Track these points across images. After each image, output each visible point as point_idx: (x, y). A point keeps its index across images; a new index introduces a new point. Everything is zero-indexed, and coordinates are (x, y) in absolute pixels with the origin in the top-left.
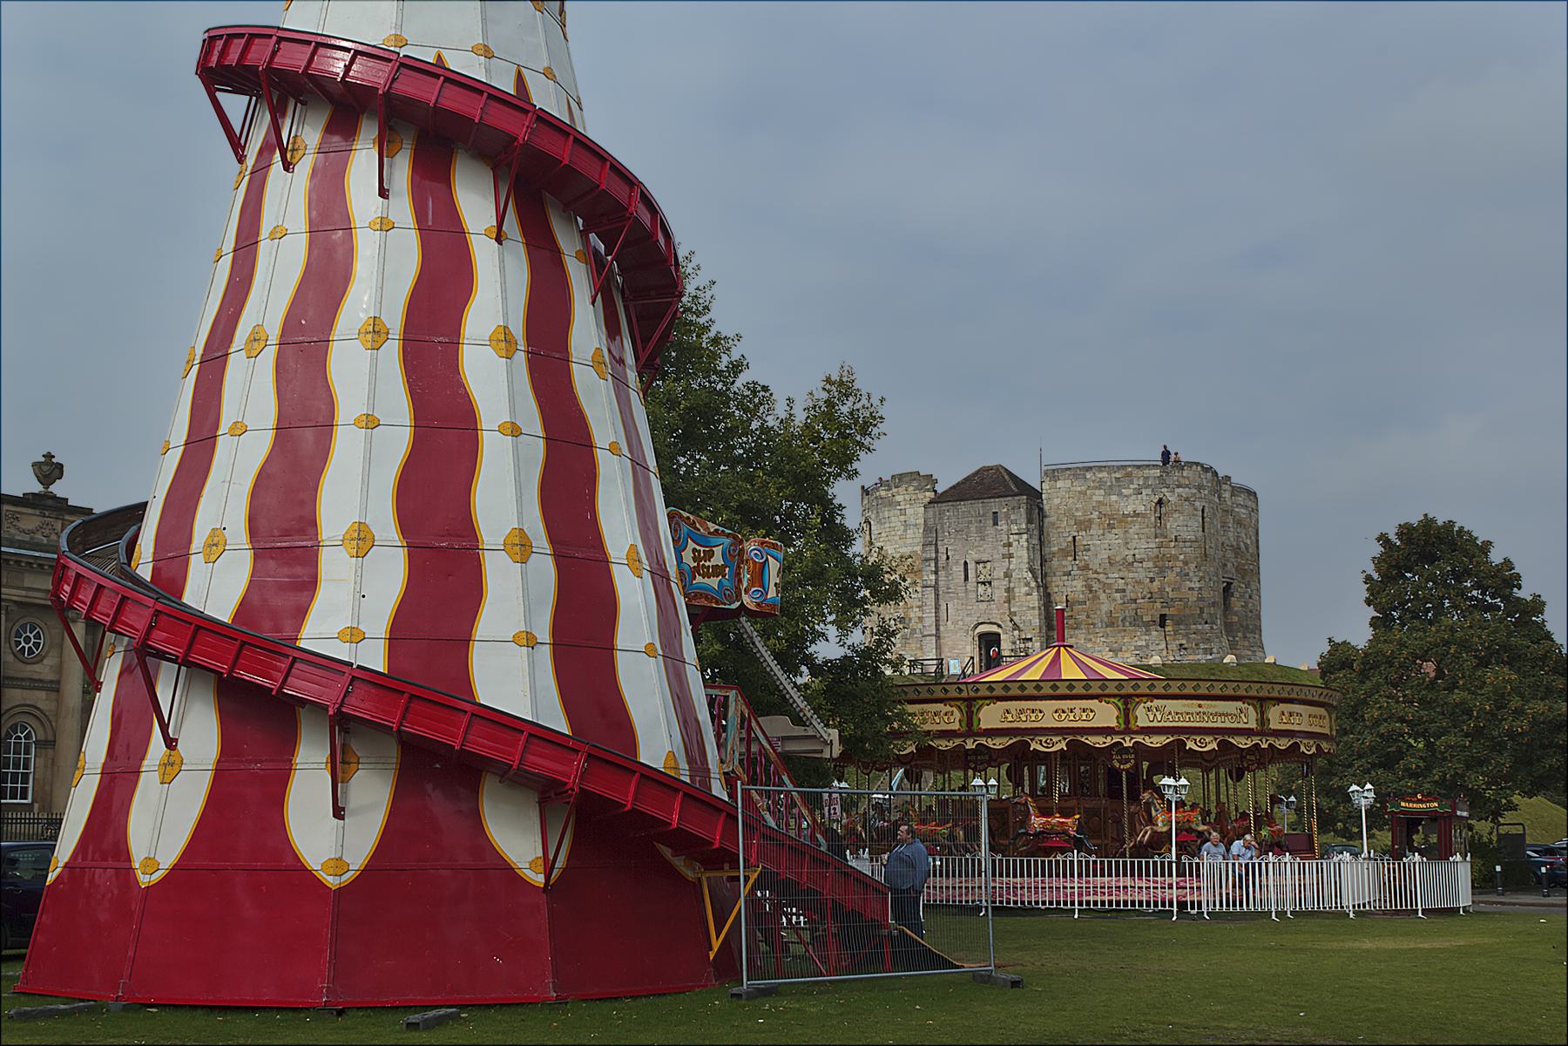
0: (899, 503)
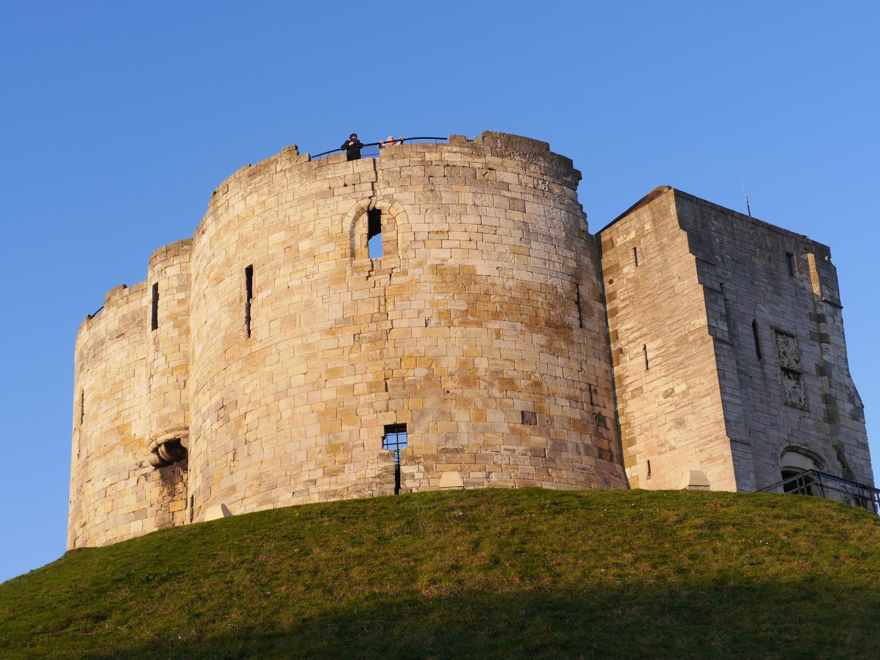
0: (506, 186)
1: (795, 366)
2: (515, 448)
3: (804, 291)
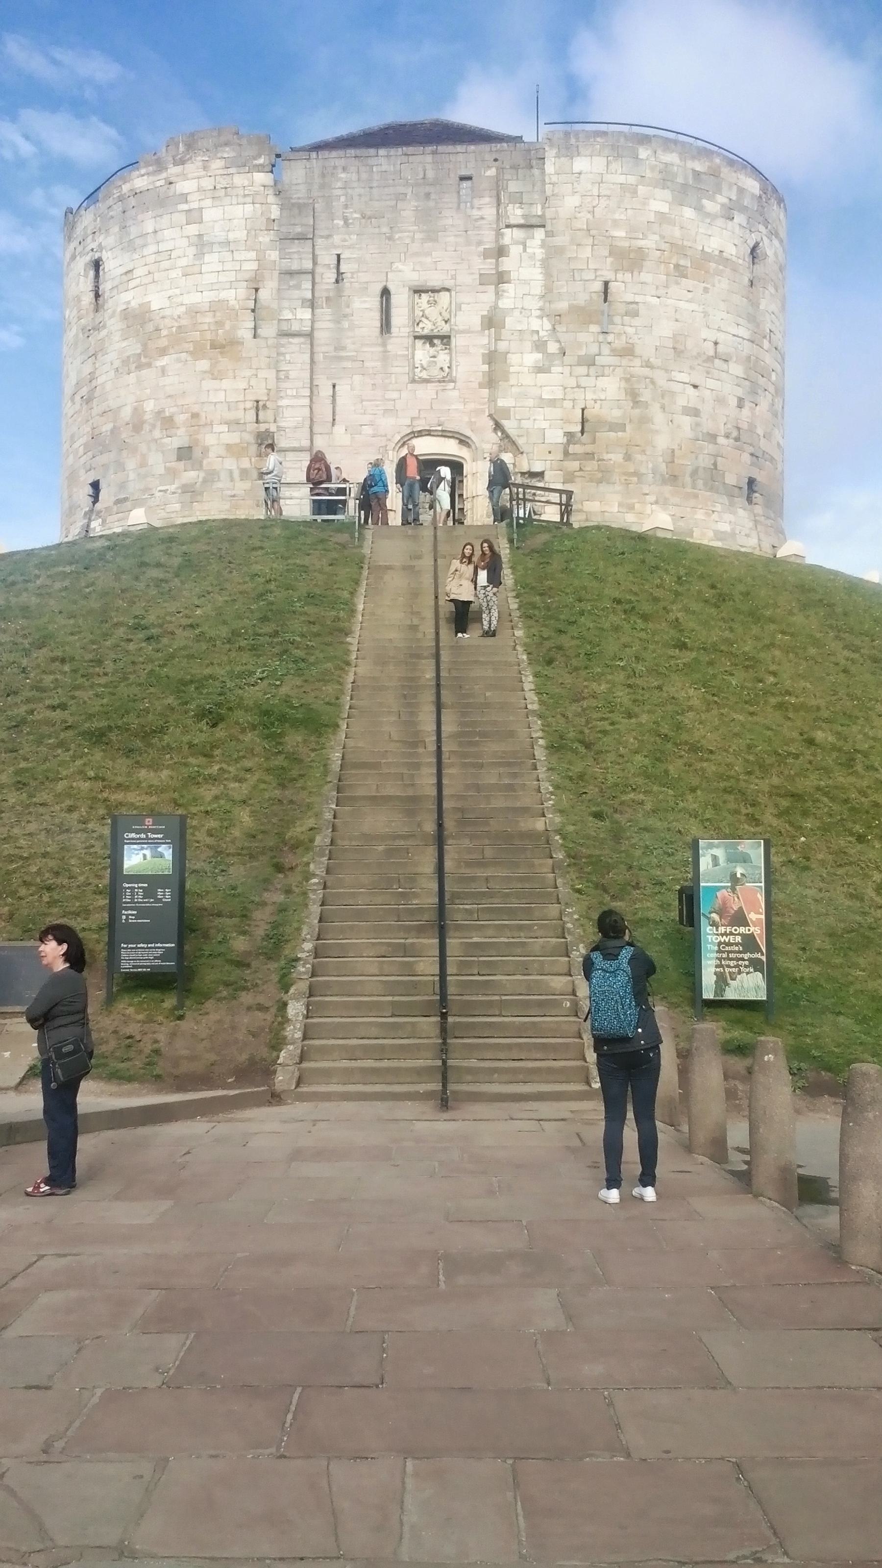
0: (184, 198)
1: (445, 329)
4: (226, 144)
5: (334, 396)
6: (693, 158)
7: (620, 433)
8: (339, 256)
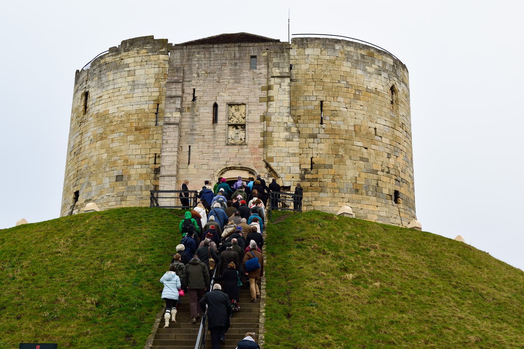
0: (128, 65)
1: (242, 121)
2: (110, 194)
3: (261, 75)
4: (148, 43)
5: (189, 151)
6: (361, 49)
7: (329, 169)
8: (194, 89)
